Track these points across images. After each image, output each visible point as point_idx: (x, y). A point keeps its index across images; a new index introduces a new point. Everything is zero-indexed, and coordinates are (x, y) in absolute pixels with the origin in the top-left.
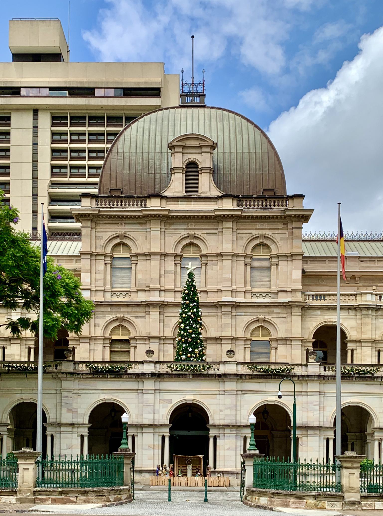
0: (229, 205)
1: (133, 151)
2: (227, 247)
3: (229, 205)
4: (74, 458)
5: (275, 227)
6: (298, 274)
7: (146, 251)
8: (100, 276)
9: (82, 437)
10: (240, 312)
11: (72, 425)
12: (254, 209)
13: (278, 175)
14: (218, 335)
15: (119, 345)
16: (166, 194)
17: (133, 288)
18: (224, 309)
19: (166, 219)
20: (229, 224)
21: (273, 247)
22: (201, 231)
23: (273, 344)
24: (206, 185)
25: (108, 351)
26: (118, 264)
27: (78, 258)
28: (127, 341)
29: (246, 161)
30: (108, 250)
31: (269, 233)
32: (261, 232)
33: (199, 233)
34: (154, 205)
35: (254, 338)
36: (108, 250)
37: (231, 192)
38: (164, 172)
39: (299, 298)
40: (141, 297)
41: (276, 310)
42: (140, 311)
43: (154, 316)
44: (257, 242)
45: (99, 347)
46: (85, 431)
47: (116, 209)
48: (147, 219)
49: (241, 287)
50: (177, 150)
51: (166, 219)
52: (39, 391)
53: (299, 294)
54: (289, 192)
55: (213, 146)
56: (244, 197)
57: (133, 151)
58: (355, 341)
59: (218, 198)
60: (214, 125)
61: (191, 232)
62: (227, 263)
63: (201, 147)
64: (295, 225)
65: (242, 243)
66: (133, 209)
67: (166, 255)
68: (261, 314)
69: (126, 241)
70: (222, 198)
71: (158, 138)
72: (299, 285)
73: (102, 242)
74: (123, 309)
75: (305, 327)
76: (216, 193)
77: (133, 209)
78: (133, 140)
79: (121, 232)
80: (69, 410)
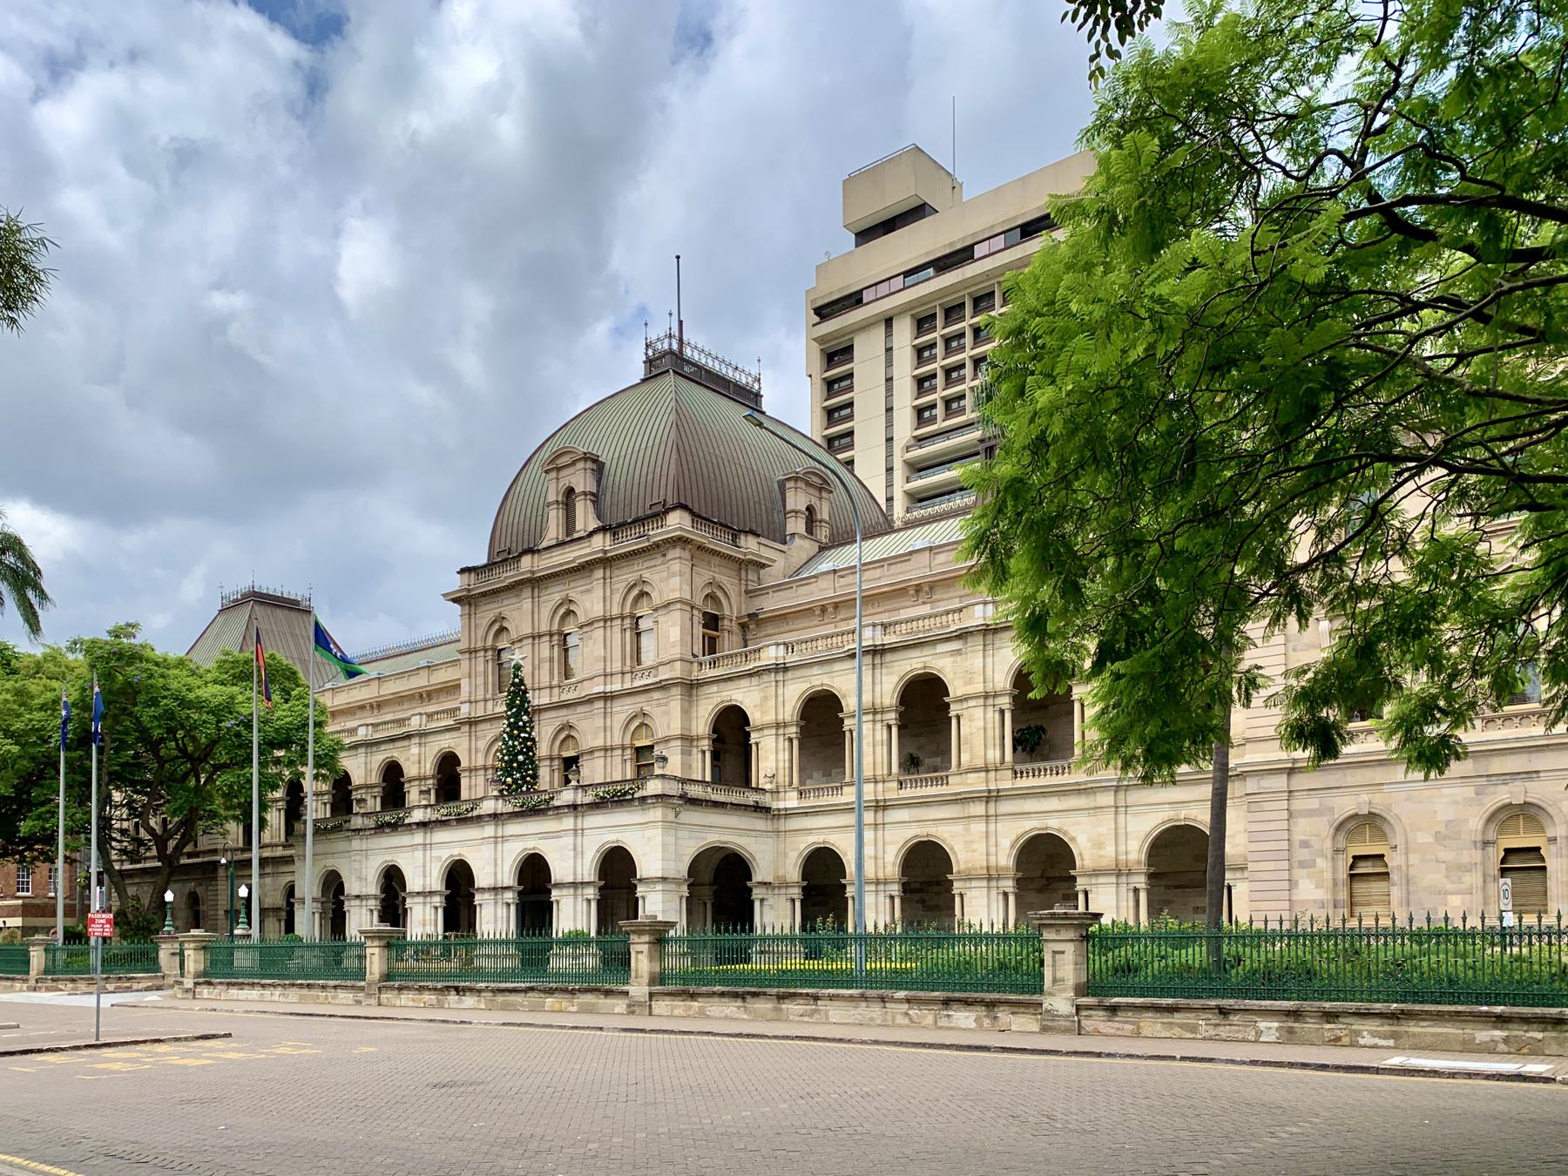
2: (597, 610)
5: (652, 563)
8: (480, 680)
19: (536, 583)
24: (585, 518)
35: (638, 744)
41: (656, 695)
45: (481, 780)
51: (536, 583)
56: (620, 525)
65: (617, 597)
73: (481, 632)
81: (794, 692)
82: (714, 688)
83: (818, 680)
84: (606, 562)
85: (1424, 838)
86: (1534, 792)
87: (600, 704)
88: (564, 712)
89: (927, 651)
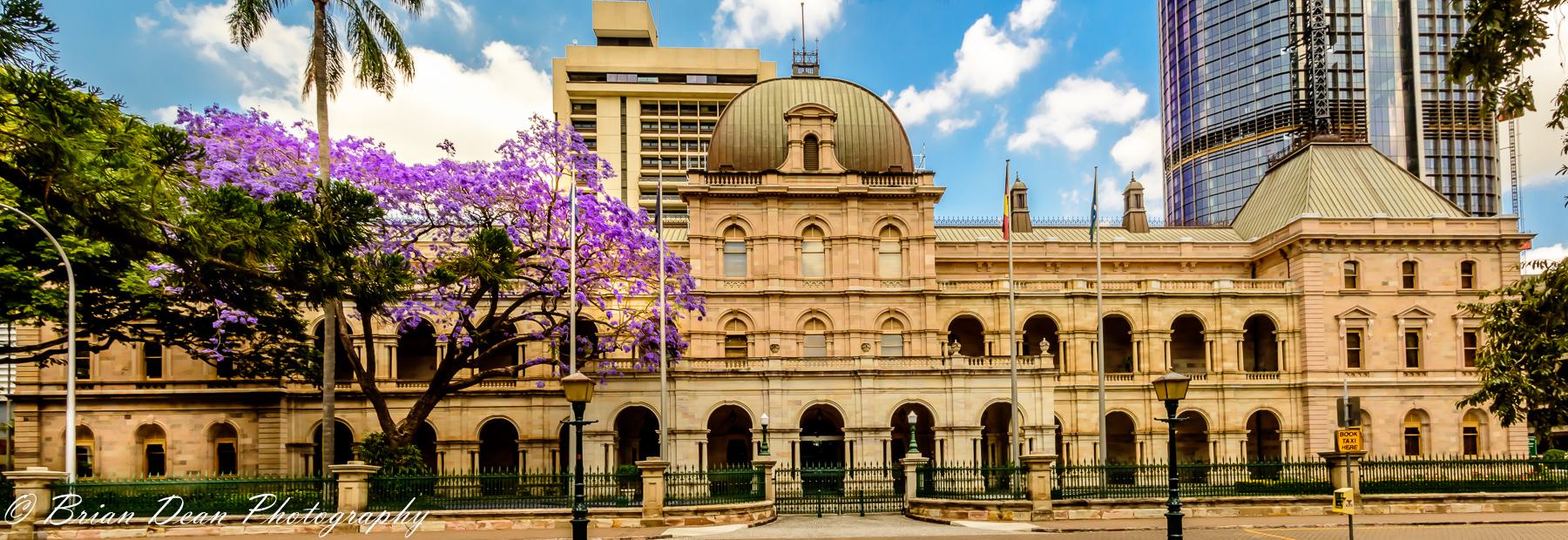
0: (854, 183)
1: (744, 123)
2: (853, 230)
3: (854, 183)
4: (689, 469)
6: (930, 260)
7: (763, 235)
9: (701, 445)
10: (869, 303)
11: (689, 432)
12: (881, 187)
13: (905, 150)
14: (846, 329)
15: (737, 344)
16: (783, 170)
17: (749, 276)
18: (852, 299)
20: (853, 204)
21: (902, 229)
22: (823, 211)
23: (907, 338)
25: (722, 347)
26: (730, 249)
27: (686, 245)
28: (744, 338)
29: (869, 135)
30: (720, 234)
31: (898, 214)
32: (890, 213)
33: (821, 214)
34: (771, 183)
36: (720, 234)
37: (856, 168)
38: (780, 145)
39: (932, 285)
40: (759, 287)
41: (908, 300)
42: (758, 302)
43: (774, 305)
44: (885, 224)
46: (704, 439)
47: (728, 187)
48: (761, 197)
49: (869, 274)
50: (794, 121)
51: (784, 197)
52: (651, 395)
53: (933, 282)
54: (917, 169)
55: (834, 118)
57: (744, 123)
58: (993, 333)
59: (840, 175)
60: (831, 96)
61: (813, 213)
62: (853, 247)
63: (820, 118)
64: (927, 204)
65: (870, 224)
66: (747, 187)
67: (785, 239)
68: (894, 304)
69: (738, 223)
70: (845, 174)
71: (771, 109)
72: (932, 272)
74: (739, 300)
75: (940, 317)
76: (839, 169)
77: (747, 187)
78: (744, 109)
79: (734, 213)
80: (685, 415)
81: (1021, 313)
82: (953, 302)
83: (1040, 308)
84: (862, 197)
85: (1382, 422)
86: (1419, 404)
87: (857, 299)
88: (812, 300)
89: (1118, 301)
